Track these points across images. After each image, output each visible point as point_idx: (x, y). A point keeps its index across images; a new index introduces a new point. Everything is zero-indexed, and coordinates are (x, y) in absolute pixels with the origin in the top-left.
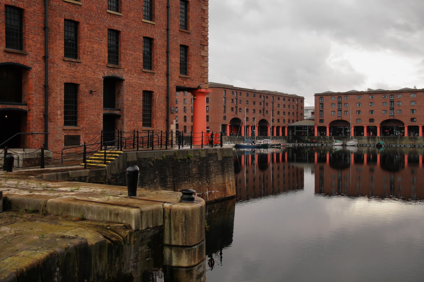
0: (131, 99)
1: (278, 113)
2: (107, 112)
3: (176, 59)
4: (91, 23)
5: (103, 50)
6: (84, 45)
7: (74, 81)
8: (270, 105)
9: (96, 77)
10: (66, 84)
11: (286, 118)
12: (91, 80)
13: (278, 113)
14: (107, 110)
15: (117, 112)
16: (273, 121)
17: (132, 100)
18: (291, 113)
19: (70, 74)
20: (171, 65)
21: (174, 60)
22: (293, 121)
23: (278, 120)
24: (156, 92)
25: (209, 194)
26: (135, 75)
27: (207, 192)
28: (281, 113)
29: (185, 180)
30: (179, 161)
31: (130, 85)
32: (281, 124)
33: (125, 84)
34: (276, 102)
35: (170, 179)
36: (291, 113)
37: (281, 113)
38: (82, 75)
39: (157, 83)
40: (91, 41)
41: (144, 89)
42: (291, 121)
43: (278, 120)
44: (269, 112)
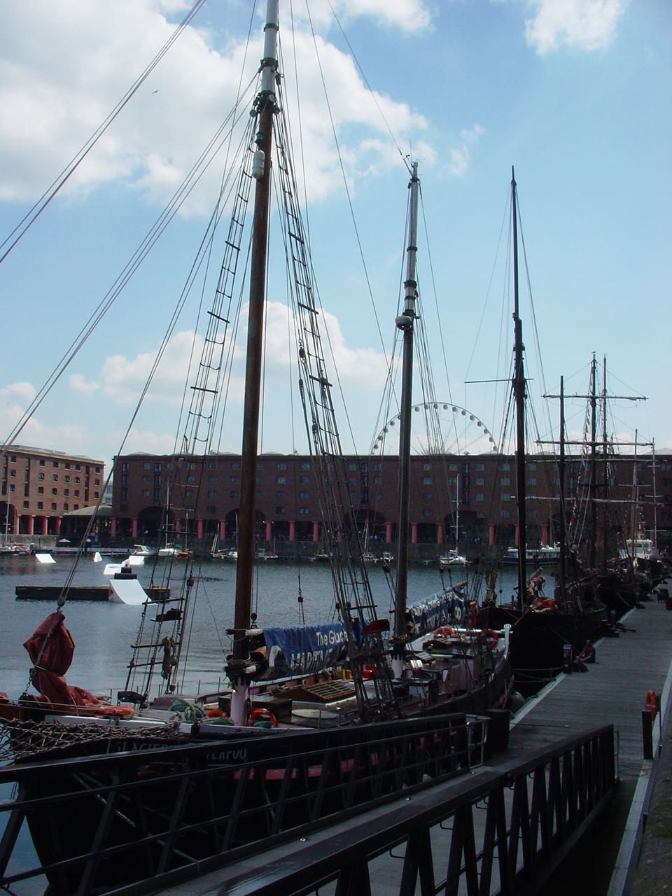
1: (41, 490)
8: (21, 475)
11: (60, 499)
13: (41, 490)
16: (26, 504)
18: (72, 493)
22: (76, 507)
23: (40, 505)
28: (48, 491)
32: (47, 512)
34: (36, 467)
36: (72, 493)
37: (48, 491)
42: (71, 507)
43: (40, 505)
44: (17, 488)
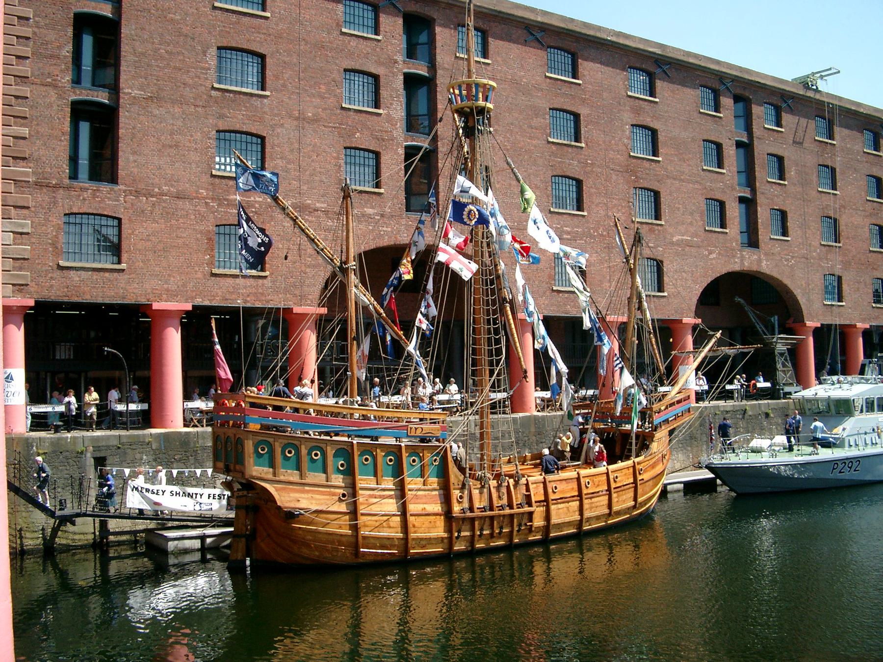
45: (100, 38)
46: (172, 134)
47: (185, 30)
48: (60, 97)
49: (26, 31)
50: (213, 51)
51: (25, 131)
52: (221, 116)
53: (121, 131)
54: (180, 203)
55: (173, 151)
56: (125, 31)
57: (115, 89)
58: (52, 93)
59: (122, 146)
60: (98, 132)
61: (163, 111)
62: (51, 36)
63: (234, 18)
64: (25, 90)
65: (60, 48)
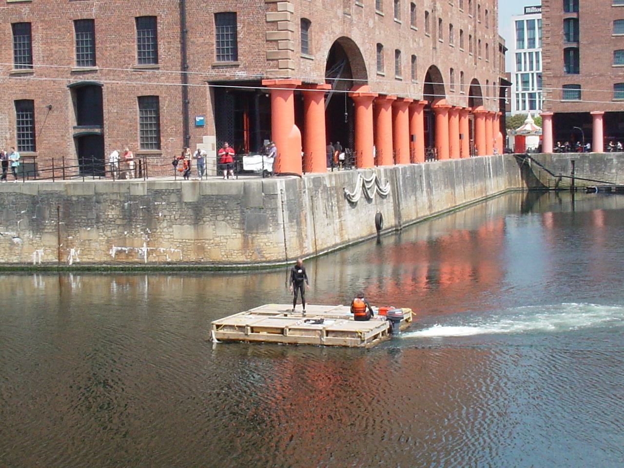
0: (115, 111)
2: (83, 131)
3: (205, 39)
4: (46, 19)
5: (67, 50)
6: (38, 48)
7: (27, 97)
9: (57, 87)
10: (15, 101)
12: (51, 92)
14: (83, 128)
15: (97, 131)
17: (117, 112)
19: (21, 88)
20: (191, 50)
21: (201, 40)
24: (164, 95)
25: (149, 253)
26: (122, 75)
27: (145, 249)
29: (87, 226)
30: (74, 199)
31: (114, 91)
33: (105, 90)
35: (50, 224)
38: (36, 88)
39: (163, 81)
40: (47, 42)
41: (140, 95)
45: (572, 27)
46: (597, 54)
47: (602, 17)
48: (560, 48)
49: (549, 29)
50: (612, 23)
51: (550, 61)
52: (615, 45)
53: (580, 56)
54: (601, 78)
55: (598, 60)
56: (580, 22)
57: (578, 42)
58: (558, 47)
59: (580, 61)
60: (572, 59)
61: (594, 47)
62: (556, 29)
63: (620, 9)
64: (548, 48)
65: (559, 32)
